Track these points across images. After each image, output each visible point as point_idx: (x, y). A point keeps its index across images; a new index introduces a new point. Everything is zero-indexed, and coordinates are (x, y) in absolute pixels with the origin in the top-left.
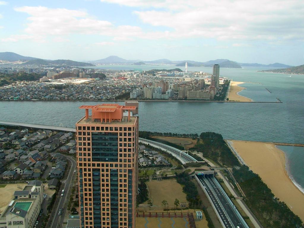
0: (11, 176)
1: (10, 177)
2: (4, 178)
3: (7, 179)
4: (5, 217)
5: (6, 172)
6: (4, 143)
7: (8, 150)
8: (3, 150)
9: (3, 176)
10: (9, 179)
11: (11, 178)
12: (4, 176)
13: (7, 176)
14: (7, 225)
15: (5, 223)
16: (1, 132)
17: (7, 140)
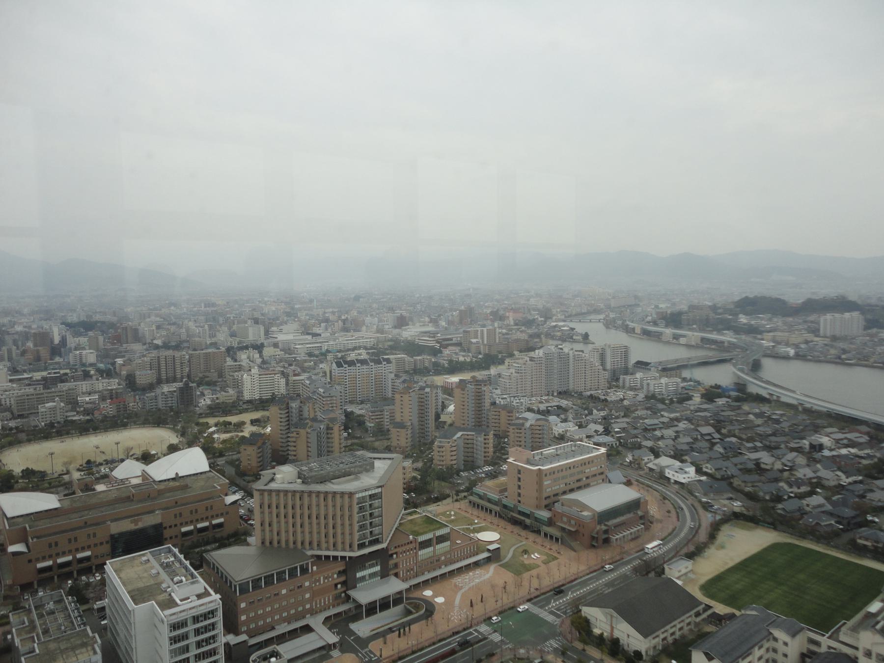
0: (877, 542)
1: (875, 544)
2: (859, 541)
3: (865, 546)
4: (858, 633)
5: (863, 529)
6: (865, 462)
7: (875, 482)
8: (860, 478)
9: (858, 536)
10: (872, 548)
11: (876, 547)
12: (860, 538)
13: (867, 539)
14: (860, 655)
15: (857, 649)
16: (860, 435)
17: (875, 456)
